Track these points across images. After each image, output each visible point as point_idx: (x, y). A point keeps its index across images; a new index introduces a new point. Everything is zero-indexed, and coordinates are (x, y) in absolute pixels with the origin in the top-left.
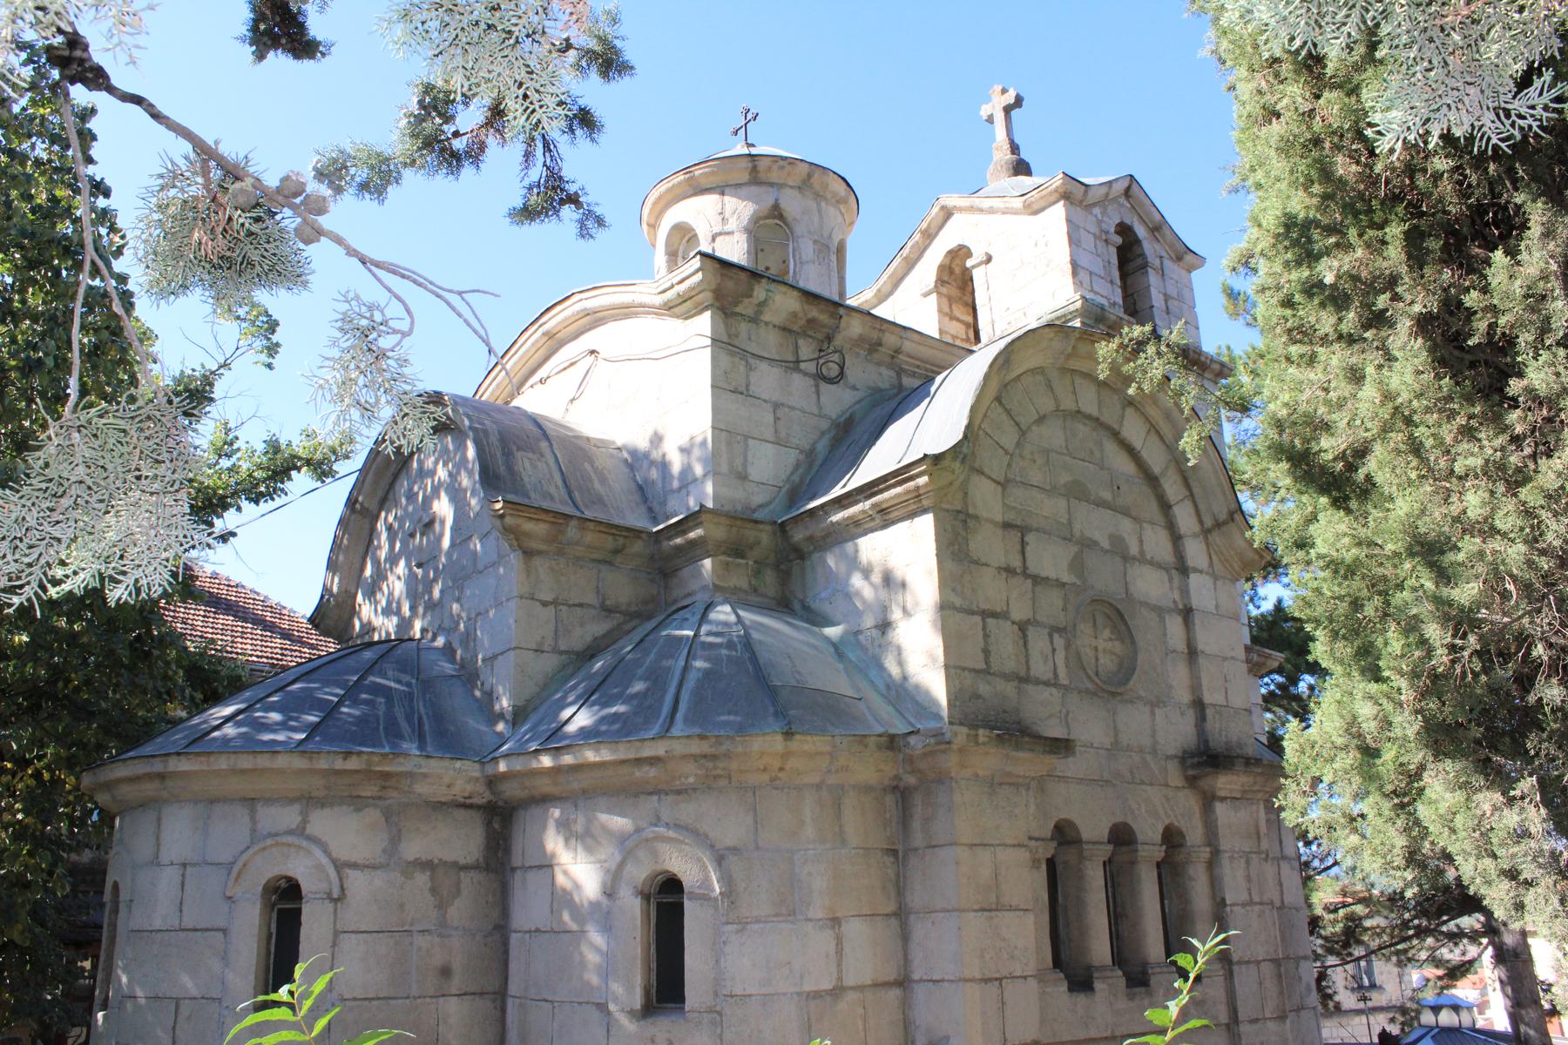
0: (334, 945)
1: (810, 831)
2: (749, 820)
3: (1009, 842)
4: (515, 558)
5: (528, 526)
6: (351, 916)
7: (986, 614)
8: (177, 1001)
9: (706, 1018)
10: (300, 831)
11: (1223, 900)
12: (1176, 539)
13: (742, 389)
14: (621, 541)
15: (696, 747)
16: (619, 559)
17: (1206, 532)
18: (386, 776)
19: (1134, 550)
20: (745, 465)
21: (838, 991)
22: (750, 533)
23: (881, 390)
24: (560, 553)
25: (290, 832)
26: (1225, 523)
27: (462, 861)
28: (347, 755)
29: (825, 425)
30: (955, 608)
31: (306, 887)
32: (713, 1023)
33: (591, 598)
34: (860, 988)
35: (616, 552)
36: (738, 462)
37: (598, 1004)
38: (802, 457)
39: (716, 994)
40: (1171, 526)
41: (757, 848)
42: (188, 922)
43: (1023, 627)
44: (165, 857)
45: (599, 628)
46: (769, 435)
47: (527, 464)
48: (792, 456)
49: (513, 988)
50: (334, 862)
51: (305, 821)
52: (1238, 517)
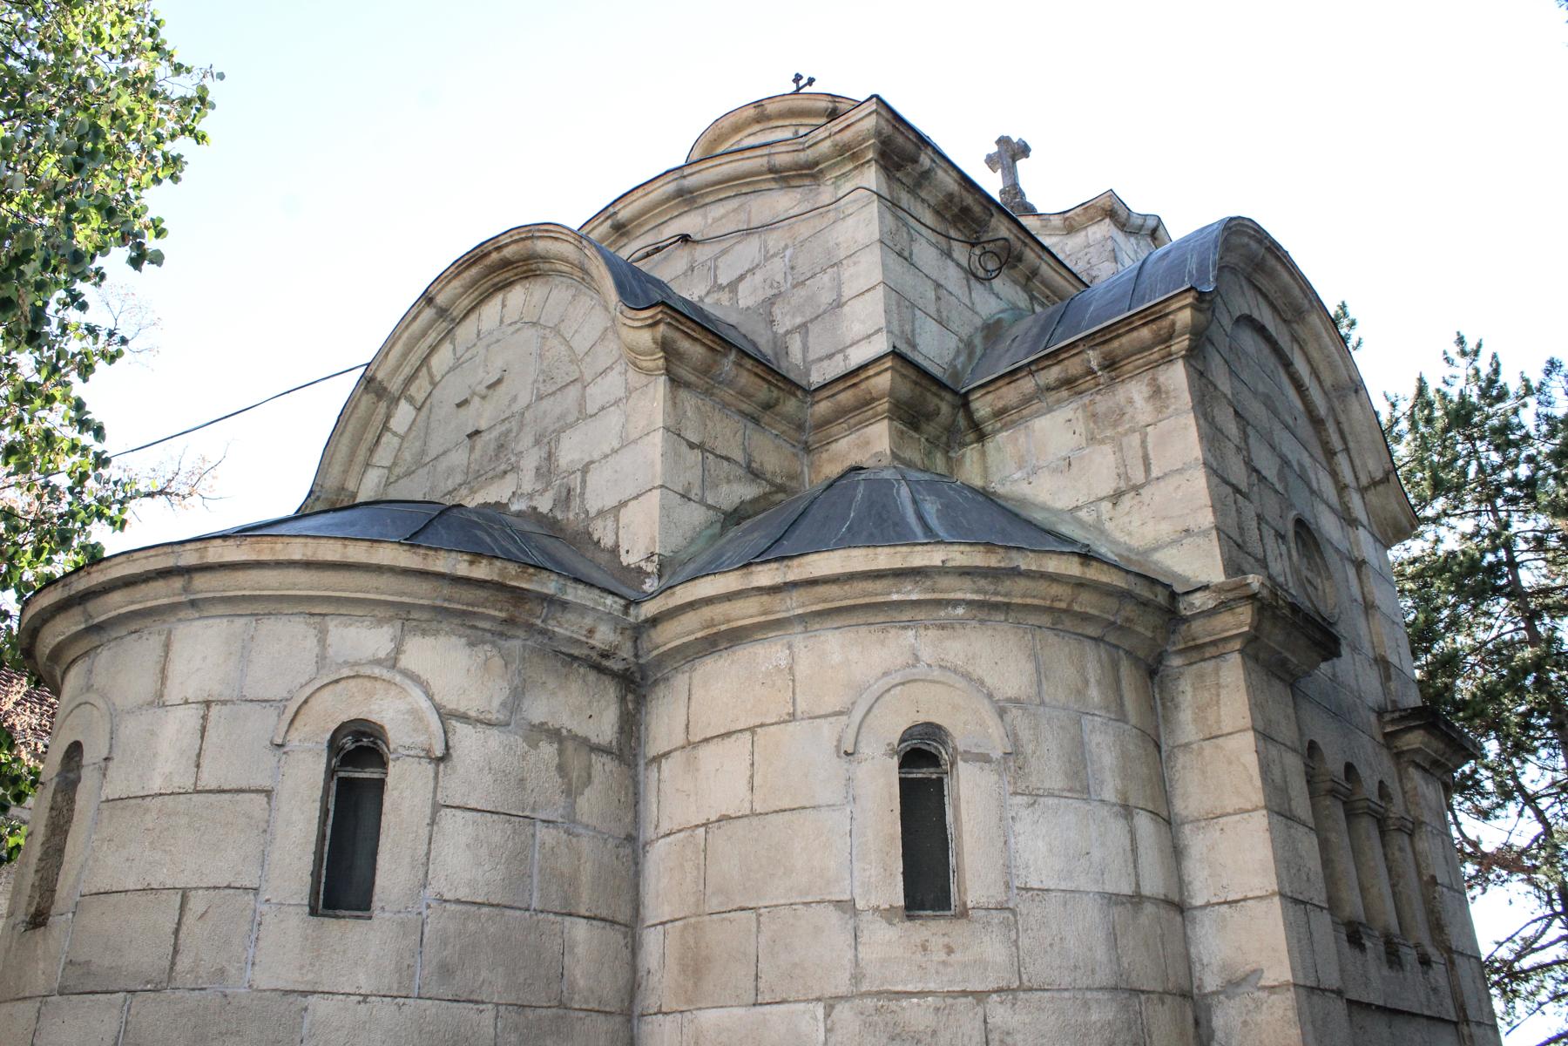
0: (433, 822)
1: (1094, 693)
2: (1030, 667)
4: (660, 387)
5: (685, 345)
6: (455, 787)
7: (1237, 490)
8: (185, 894)
9: (997, 917)
10: (392, 662)
11: (1433, 878)
12: (1342, 488)
13: (906, 254)
14: (776, 393)
16: (766, 418)
17: (1363, 491)
18: (519, 596)
19: (1315, 486)
21: (1136, 899)
24: (708, 393)
25: (378, 662)
26: (1381, 482)
27: (594, 740)
28: (476, 556)
29: (978, 322)
31: (398, 735)
32: (1005, 924)
34: (1154, 900)
35: (768, 406)
36: (908, 328)
37: (838, 904)
38: (961, 346)
39: (1007, 886)
40: (1334, 474)
41: (1042, 703)
42: (208, 779)
43: (1260, 518)
44: (173, 694)
45: (748, 491)
46: (932, 310)
48: (952, 343)
50: (438, 708)
51: (398, 650)
52: (1392, 477)
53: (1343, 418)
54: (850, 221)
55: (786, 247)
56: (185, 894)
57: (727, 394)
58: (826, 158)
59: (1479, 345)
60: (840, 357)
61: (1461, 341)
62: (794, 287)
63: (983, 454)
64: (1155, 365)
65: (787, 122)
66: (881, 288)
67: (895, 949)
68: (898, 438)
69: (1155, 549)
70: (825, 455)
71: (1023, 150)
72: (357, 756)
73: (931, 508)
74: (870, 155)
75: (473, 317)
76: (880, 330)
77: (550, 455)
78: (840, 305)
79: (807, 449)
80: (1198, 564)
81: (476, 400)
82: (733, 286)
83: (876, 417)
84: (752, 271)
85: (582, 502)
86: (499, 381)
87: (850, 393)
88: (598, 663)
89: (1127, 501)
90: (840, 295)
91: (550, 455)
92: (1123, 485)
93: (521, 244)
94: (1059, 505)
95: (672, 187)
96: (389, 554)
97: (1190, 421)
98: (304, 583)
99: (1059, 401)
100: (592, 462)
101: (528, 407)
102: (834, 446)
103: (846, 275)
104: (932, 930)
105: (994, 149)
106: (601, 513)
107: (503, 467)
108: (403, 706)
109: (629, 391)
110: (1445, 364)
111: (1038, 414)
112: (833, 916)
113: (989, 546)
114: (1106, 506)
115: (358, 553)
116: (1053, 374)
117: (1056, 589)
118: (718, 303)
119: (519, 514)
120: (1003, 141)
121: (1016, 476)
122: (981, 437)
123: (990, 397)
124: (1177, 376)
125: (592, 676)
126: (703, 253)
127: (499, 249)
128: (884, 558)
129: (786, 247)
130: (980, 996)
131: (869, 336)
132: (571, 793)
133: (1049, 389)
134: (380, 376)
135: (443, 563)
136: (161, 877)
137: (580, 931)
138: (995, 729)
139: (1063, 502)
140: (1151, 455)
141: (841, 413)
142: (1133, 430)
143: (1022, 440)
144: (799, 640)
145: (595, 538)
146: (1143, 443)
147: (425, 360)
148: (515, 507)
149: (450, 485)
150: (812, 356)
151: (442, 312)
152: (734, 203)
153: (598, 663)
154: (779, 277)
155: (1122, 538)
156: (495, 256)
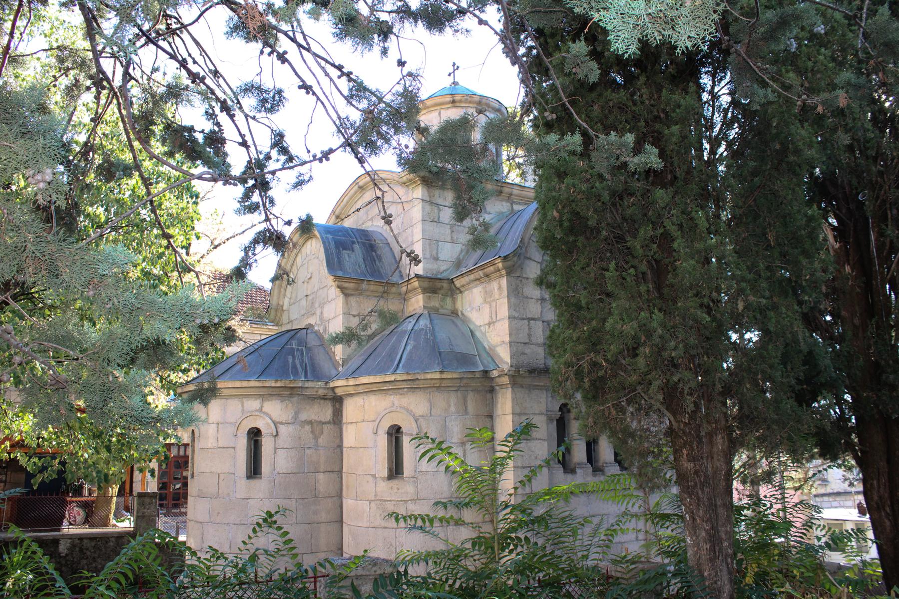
1: (453, 409)
2: (428, 405)
3: (537, 412)
4: (341, 297)
5: (346, 285)
6: (281, 442)
8: (219, 474)
9: (412, 480)
10: (261, 410)
20: (437, 254)
22: (438, 284)
23: (503, 213)
24: (360, 294)
25: (257, 411)
28: (276, 381)
30: (515, 318)
32: (414, 482)
36: (434, 253)
42: (221, 445)
44: (211, 421)
46: (448, 239)
47: (346, 256)
49: (344, 470)
51: (262, 406)
56: (219, 474)
57: (368, 293)
66: (421, 242)
67: (384, 488)
72: (255, 434)
80: (504, 355)
88: (324, 398)
96: (253, 384)
97: (506, 300)
98: (234, 392)
104: (394, 483)
108: (264, 422)
112: (371, 479)
115: (245, 384)
117: (433, 381)
125: (322, 401)
128: (378, 379)
130: (406, 502)
132: (316, 438)
135: (267, 384)
136: (213, 470)
137: (321, 476)
138: (414, 425)
142: (494, 300)
153: (324, 398)
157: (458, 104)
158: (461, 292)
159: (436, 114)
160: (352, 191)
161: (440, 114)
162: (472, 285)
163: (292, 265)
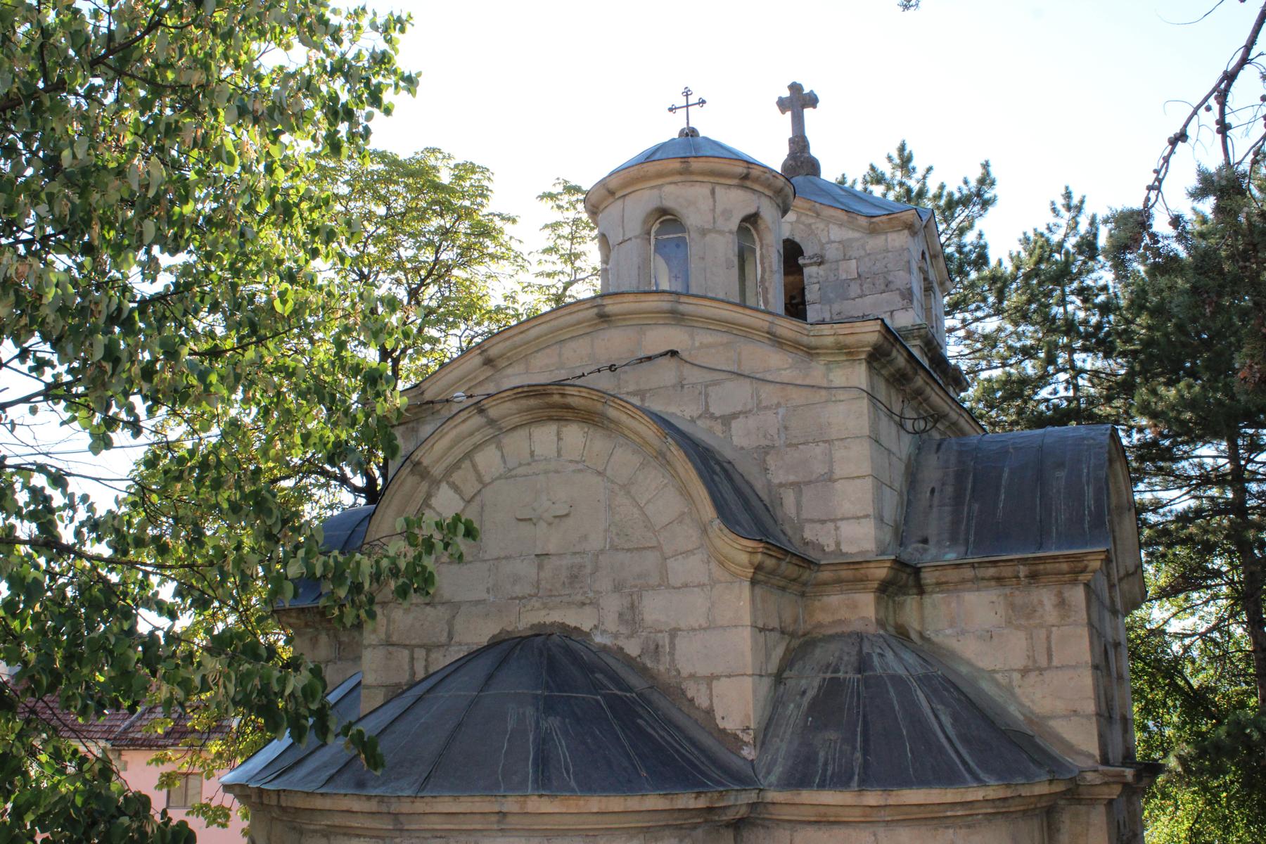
15: (1001, 793)
28: (699, 794)
33: (777, 626)
53: (1117, 529)
54: (842, 407)
55: (778, 405)
58: (827, 348)
59: (1082, 202)
60: (831, 525)
61: (1068, 195)
62: (790, 445)
63: (921, 607)
64: (1065, 583)
65: (706, 179)
68: (878, 602)
69: (1051, 718)
70: (817, 603)
71: (812, 101)
73: (946, 720)
74: (863, 356)
75: (523, 433)
76: (867, 516)
77: (633, 607)
78: (832, 480)
79: (803, 595)
81: (543, 525)
82: (727, 420)
83: (865, 589)
84: (745, 413)
85: (673, 660)
86: (567, 515)
87: (850, 572)
89: (1033, 676)
90: (831, 471)
91: (633, 607)
92: (1030, 664)
93: (590, 402)
94: (980, 665)
95: (666, 306)
96: (653, 802)
97: (1085, 632)
99: (987, 588)
100: (680, 630)
101: (602, 551)
102: (825, 598)
103: (839, 454)
105: (786, 93)
106: (692, 676)
107: (579, 598)
109: (714, 582)
110: (1052, 214)
111: (969, 590)
113: (1008, 786)
114: (1016, 676)
116: (992, 571)
118: (710, 430)
119: (604, 648)
120: (795, 88)
121: (948, 632)
122: (921, 591)
123: (937, 573)
124: (1077, 595)
126: (693, 376)
127: (563, 395)
129: (778, 405)
131: (858, 518)
133: (983, 579)
134: (426, 462)
139: (985, 663)
140: (1054, 648)
141: (840, 581)
142: (1041, 626)
143: (953, 605)
144: (881, 831)
145: (690, 695)
146: (1048, 638)
147: (468, 455)
148: (599, 639)
149: (518, 590)
150: (805, 515)
151: (492, 422)
152: (725, 338)
154: (773, 431)
155: (1028, 703)
156: (556, 398)
157: (748, 183)
158: (921, 591)
159: (704, 190)
160: (575, 318)
161: (713, 192)
162: (969, 585)
163: (456, 466)
